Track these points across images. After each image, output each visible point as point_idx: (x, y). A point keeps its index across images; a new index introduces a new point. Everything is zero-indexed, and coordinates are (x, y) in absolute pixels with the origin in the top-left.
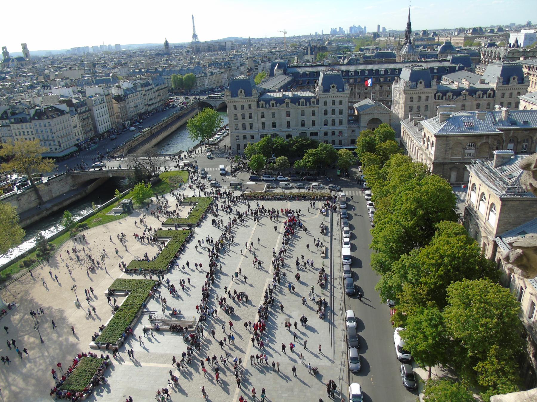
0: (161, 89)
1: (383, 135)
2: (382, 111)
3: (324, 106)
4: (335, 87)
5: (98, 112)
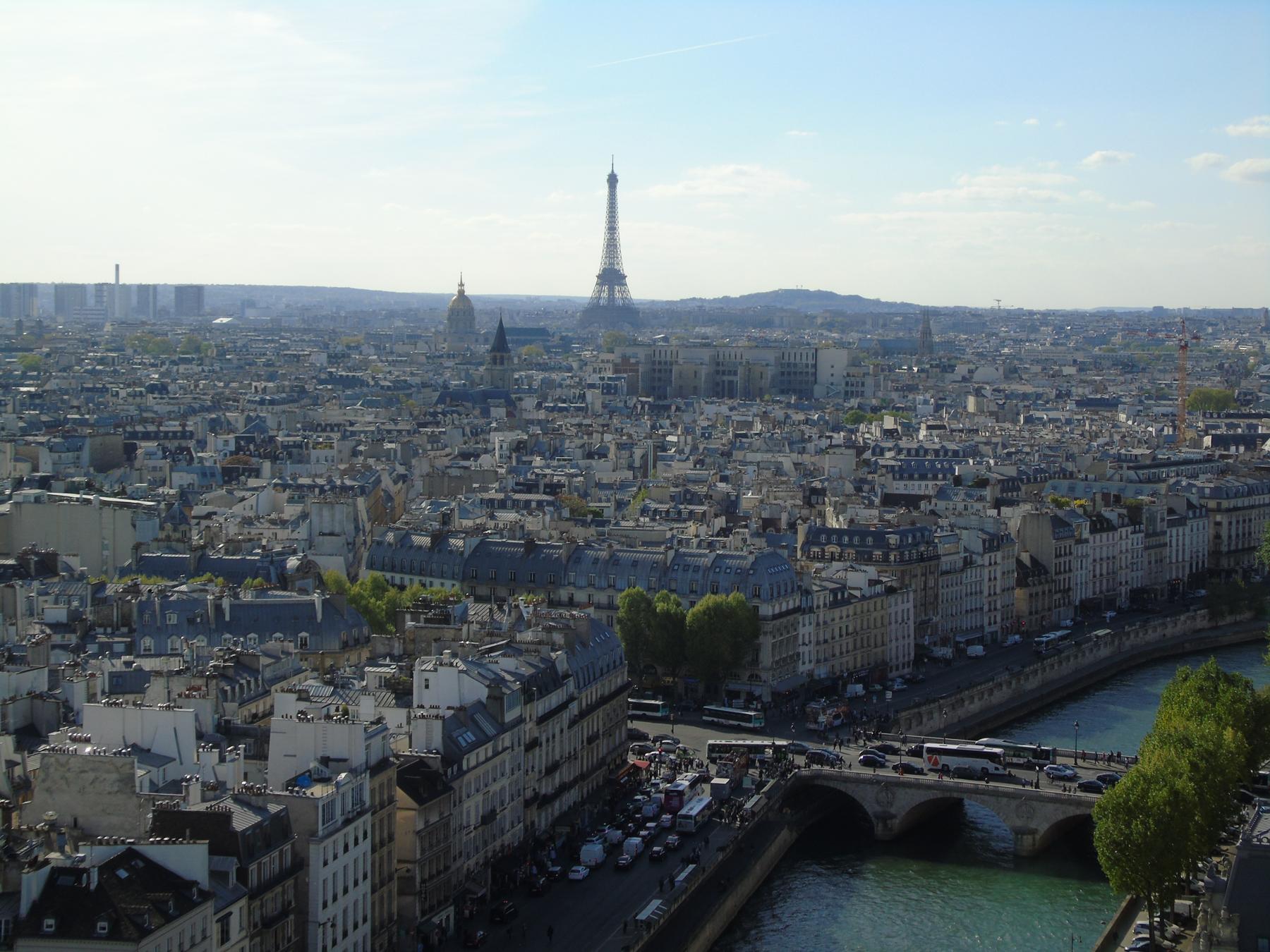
0: (604, 700)
5: (326, 873)
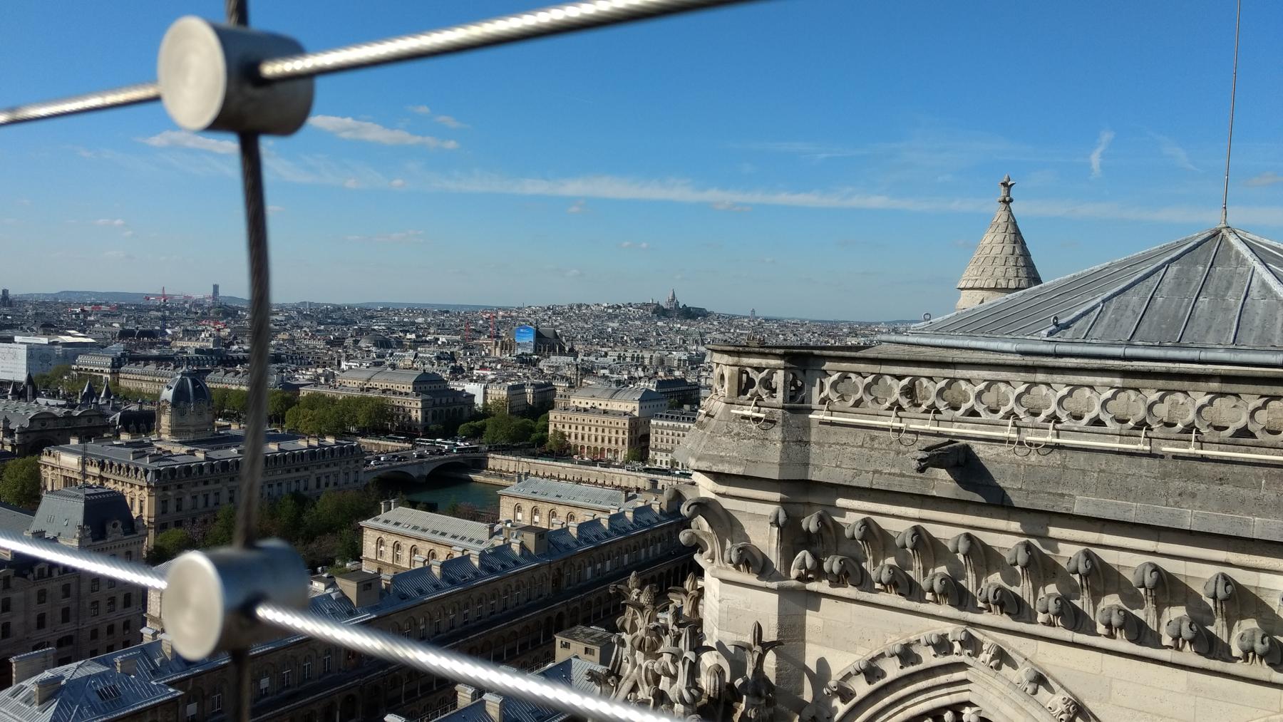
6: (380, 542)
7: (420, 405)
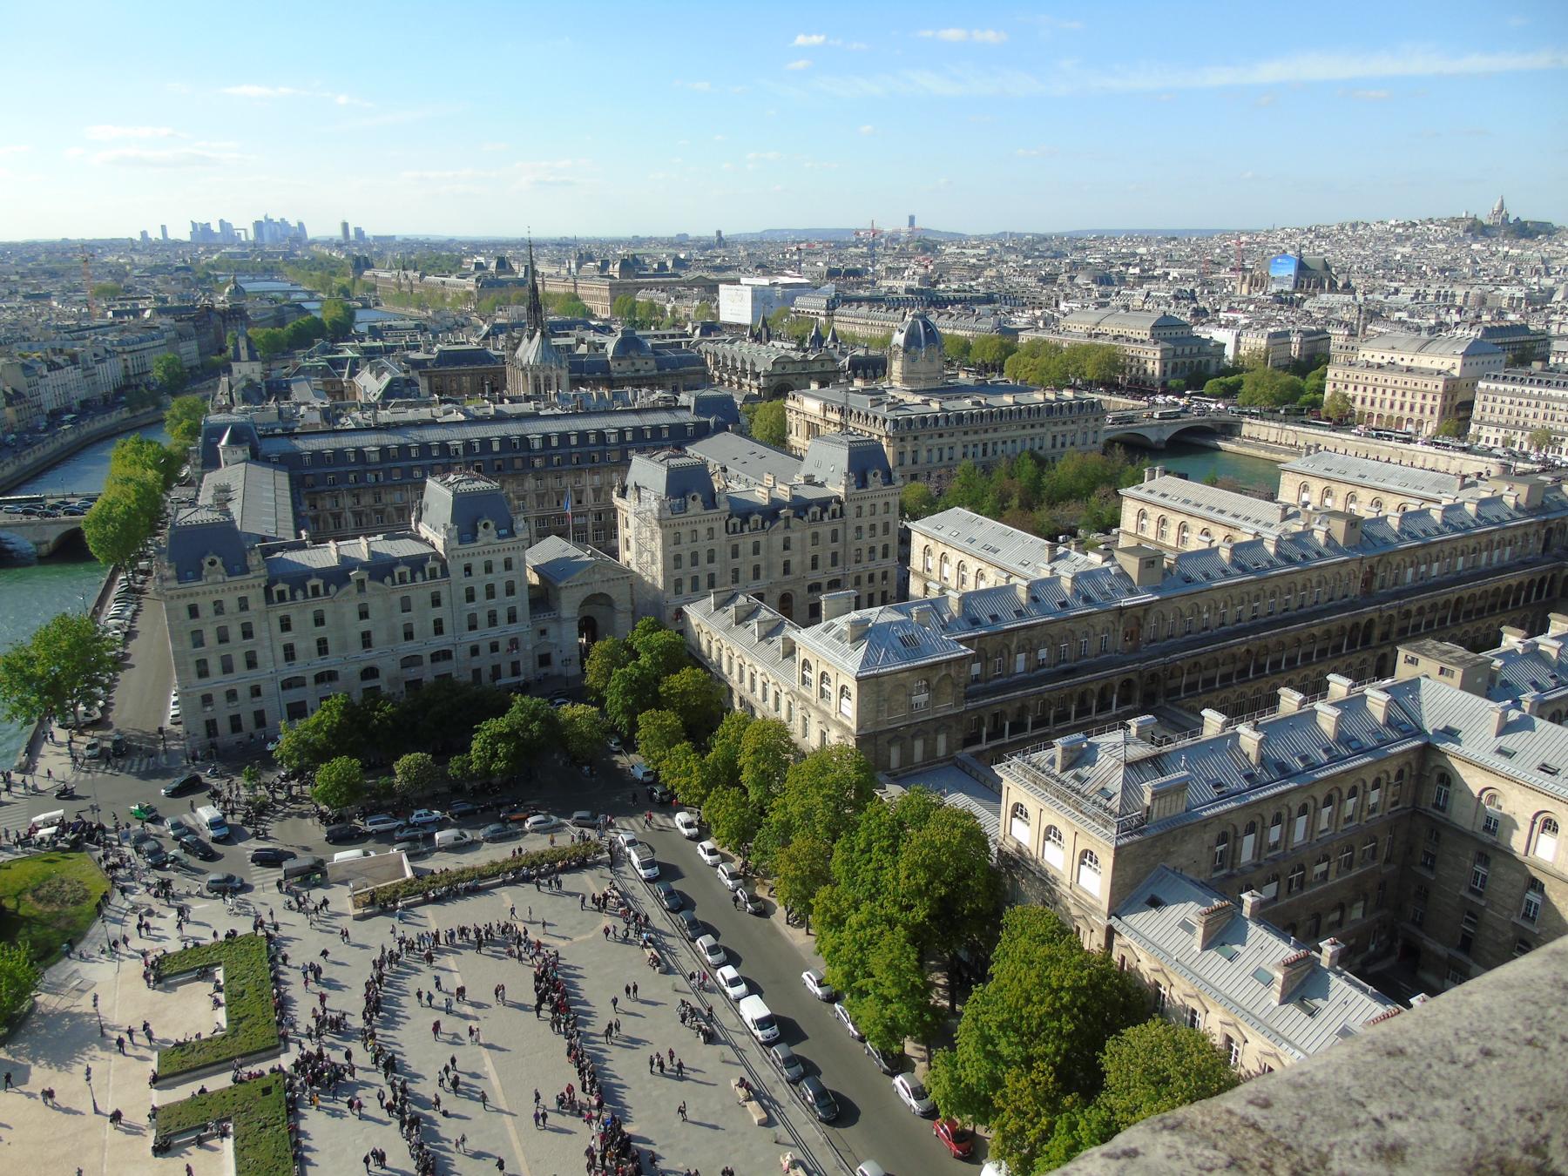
1: (661, 653)
2: (611, 575)
3: (465, 580)
4: (492, 525)
6: (1142, 515)
7: (1158, 355)
